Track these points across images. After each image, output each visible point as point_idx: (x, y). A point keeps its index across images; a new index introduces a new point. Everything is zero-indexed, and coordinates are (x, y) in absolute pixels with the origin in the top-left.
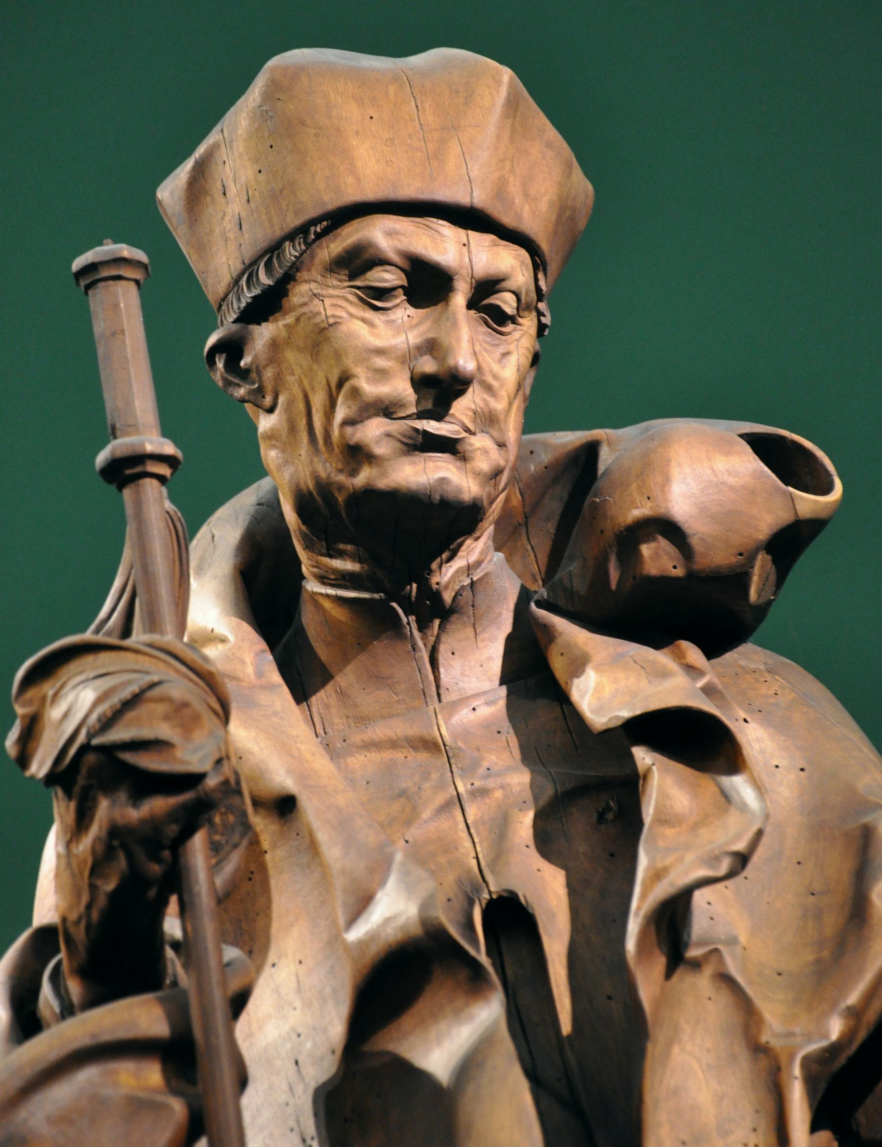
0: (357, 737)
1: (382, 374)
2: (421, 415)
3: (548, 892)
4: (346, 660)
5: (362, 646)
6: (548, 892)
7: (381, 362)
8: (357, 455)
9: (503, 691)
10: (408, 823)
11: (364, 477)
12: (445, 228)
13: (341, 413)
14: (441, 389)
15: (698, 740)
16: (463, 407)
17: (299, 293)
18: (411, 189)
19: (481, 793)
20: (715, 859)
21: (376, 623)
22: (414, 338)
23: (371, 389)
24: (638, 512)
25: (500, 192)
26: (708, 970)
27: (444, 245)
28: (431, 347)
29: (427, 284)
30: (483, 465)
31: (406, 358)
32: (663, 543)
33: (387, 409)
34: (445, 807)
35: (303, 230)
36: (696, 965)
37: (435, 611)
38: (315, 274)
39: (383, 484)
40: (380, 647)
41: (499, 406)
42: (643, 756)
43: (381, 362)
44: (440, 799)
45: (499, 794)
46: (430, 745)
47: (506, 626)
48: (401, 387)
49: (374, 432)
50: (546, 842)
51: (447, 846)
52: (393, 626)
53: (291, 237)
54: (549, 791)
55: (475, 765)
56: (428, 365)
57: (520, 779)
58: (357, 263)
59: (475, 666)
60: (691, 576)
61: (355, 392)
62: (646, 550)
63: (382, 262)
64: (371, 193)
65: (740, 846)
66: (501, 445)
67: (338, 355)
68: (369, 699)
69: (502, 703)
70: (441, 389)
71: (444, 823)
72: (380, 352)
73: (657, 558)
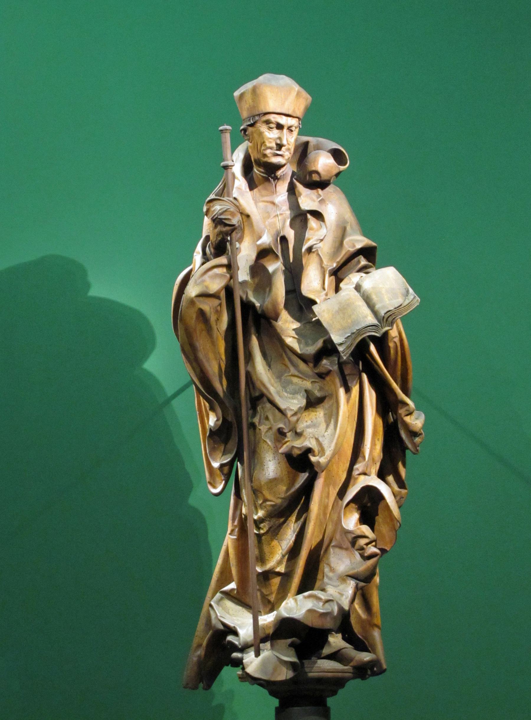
0: (261, 199)
1: (270, 142)
2: (277, 150)
3: (290, 234)
4: (260, 184)
5: (263, 183)
6: (290, 234)
7: (270, 140)
8: (265, 156)
9: (287, 193)
10: (269, 218)
11: (266, 159)
12: (284, 117)
13: (263, 148)
14: (280, 146)
15: (318, 215)
16: (283, 149)
17: (258, 125)
18: (278, 111)
19: (281, 214)
20: (318, 240)
21: (267, 180)
22: (276, 136)
23: (268, 145)
24: (314, 169)
25: (294, 111)
26: (316, 253)
27: (283, 120)
28: (280, 138)
29: (280, 127)
30: (286, 157)
31: (275, 139)
32: (316, 175)
33: (271, 148)
34: (275, 216)
35: (259, 115)
36: (314, 252)
37: (276, 178)
38: (260, 122)
39: (269, 161)
40: (267, 184)
41: (290, 147)
42: (309, 216)
43: (270, 140)
44: (274, 215)
45: (284, 215)
46: (273, 203)
47: (289, 180)
48: (274, 145)
49: (268, 152)
50: (292, 226)
51: (275, 224)
52: (269, 181)
53: (257, 115)
54: (293, 216)
55: (281, 208)
56: (278, 142)
57: (288, 212)
58: (268, 122)
59: (283, 188)
60: (320, 180)
61: (265, 145)
62: (313, 175)
63: (272, 123)
64: (271, 111)
65: (322, 238)
66: (290, 153)
67: (263, 138)
68: (264, 192)
69: (287, 196)
70: (280, 146)
71: (274, 219)
72: (270, 138)
73: (315, 178)
